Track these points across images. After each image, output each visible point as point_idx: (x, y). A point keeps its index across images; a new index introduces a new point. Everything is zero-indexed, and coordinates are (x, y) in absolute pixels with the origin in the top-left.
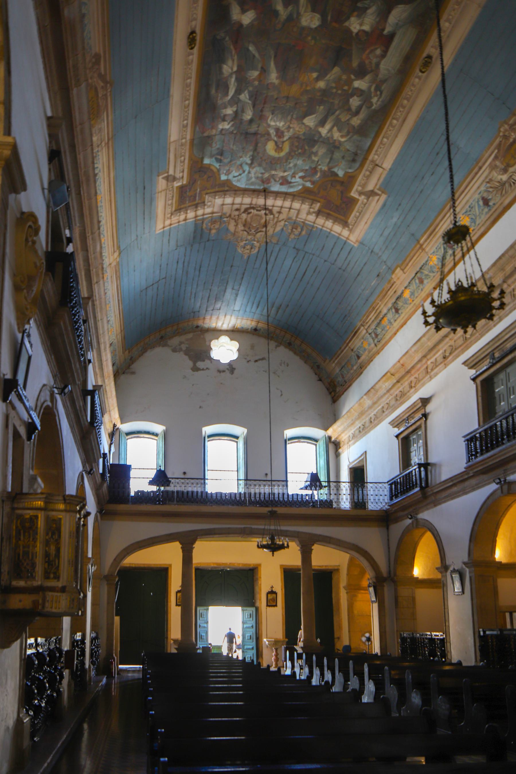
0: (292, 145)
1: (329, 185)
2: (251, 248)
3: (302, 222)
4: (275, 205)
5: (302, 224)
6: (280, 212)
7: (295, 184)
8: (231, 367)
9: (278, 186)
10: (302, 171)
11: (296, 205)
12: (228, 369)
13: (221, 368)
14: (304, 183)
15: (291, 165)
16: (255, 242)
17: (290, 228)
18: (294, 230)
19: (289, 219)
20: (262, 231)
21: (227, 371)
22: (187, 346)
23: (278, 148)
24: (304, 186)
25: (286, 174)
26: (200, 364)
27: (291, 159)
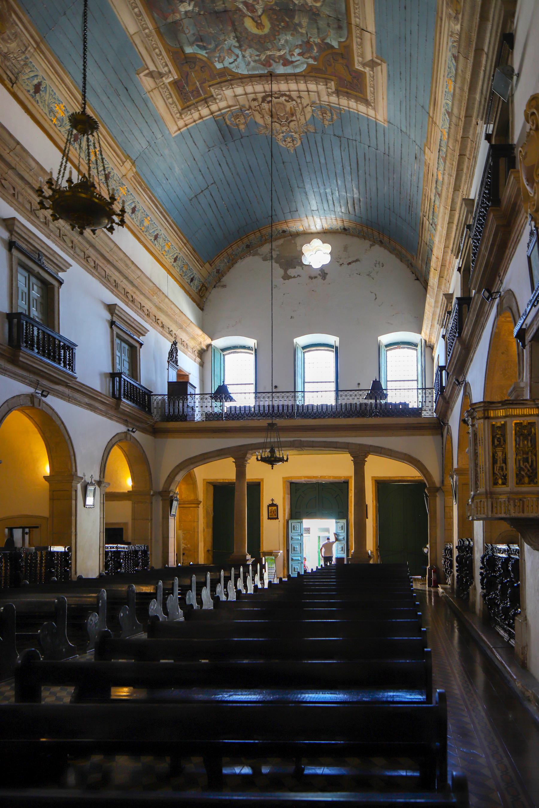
0: (270, 19)
2: (293, 141)
3: (328, 105)
8: (323, 273)
9: (282, 67)
10: (297, 47)
11: (312, 87)
12: (319, 275)
13: (313, 275)
14: (306, 60)
15: (282, 42)
16: (293, 134)
17: (319, 113)
18: (325, 115)
20: (294, 121)
21: (319, 277)
22: (278, 253)
23: (259, 25)
24: (308, 64)
25: (282, 53)
26: (291, 272)
27: (279, 35)
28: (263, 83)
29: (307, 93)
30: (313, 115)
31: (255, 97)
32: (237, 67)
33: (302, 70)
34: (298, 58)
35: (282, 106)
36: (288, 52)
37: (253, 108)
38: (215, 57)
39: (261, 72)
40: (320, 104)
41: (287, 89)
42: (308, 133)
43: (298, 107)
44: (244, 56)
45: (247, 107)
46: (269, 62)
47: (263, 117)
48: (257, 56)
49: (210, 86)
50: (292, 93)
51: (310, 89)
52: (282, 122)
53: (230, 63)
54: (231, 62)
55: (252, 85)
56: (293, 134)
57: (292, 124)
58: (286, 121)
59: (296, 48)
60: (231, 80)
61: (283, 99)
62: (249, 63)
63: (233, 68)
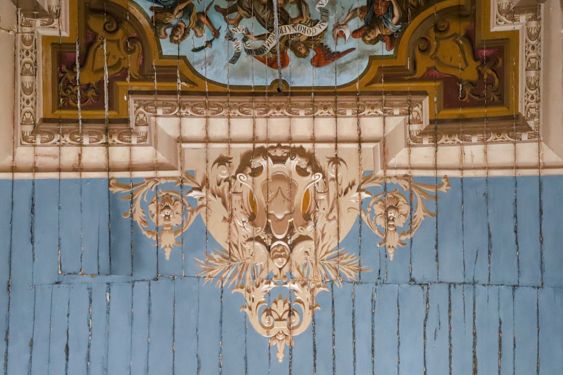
1: (432, 34)
2: (291, 312)
3: (406, 177)
4: (319, 134)
5: (403, 183)
6: (336, 160)
7: (348, 57)
9: (310, 68)
10: (354, 13)
14: (370, 47)
16: (296, 286)
17: (379, 210)
18: (392, 214)
19: (368, 177)
20: (307, 238)
24: (373, 58)
25: (317, 30)
28: (256, 112)
29: (355, 146)
30: (360, 216)
31: (225, 155)
32: (208, 62)
33: (357, 76)
34: (353, 43)
35: (285, 187)
36: (331, 29)
37: (213, 184)
38: (169, 25)
39: (259, 82)
40: (386, 177)
41: (308, 134)
42: (338, 284)
43: (327, 192)
44: (230, 37)
45: (199, 179)
46: (283, 54)
47: (230, 219)
48: (261, 37)
49: (131, 93)
50: (319, 146)
51: (366, 134)
52: (274, 239)
53: (195, 50)
54: (197, 46)
55: (229, 117)
56: (296, 286)
57: (300, 248)
58: (285, 240)
59: (353, 17)
60: (184, 93)
61: (292, 164)
62: (237, 56)
63: (199, 62)
